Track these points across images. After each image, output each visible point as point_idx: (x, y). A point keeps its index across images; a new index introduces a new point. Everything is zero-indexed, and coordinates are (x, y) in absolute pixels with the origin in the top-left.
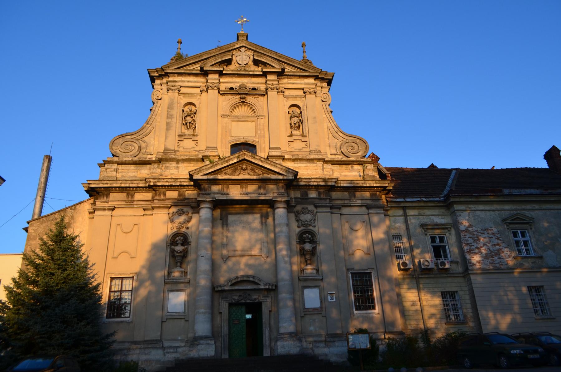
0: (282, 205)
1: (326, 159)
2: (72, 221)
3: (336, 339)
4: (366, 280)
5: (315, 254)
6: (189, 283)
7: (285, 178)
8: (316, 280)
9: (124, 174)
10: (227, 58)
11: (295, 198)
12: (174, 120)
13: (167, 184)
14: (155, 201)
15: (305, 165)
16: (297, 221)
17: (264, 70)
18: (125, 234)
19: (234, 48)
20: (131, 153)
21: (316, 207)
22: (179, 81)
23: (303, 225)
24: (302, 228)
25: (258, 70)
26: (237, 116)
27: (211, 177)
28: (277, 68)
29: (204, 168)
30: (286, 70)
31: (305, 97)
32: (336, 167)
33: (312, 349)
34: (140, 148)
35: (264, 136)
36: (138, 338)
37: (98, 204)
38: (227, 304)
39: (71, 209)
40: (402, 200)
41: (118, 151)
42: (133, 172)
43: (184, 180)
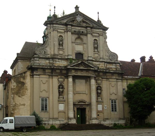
3: (106, 120)
6: (65, 101)
8: (101, 102)
16: (96, 83)
20: (42, 54)
22: (57, 27)
24: (98, 85)
25: (84, 25)
27: (73, 68)
31: (99, 37)
32: (107, 64)
33: (100, 122)
35: (86, 52)
36: (51, 116)
37: (35, 73)
40: (127, 77)
41: (37, 53)
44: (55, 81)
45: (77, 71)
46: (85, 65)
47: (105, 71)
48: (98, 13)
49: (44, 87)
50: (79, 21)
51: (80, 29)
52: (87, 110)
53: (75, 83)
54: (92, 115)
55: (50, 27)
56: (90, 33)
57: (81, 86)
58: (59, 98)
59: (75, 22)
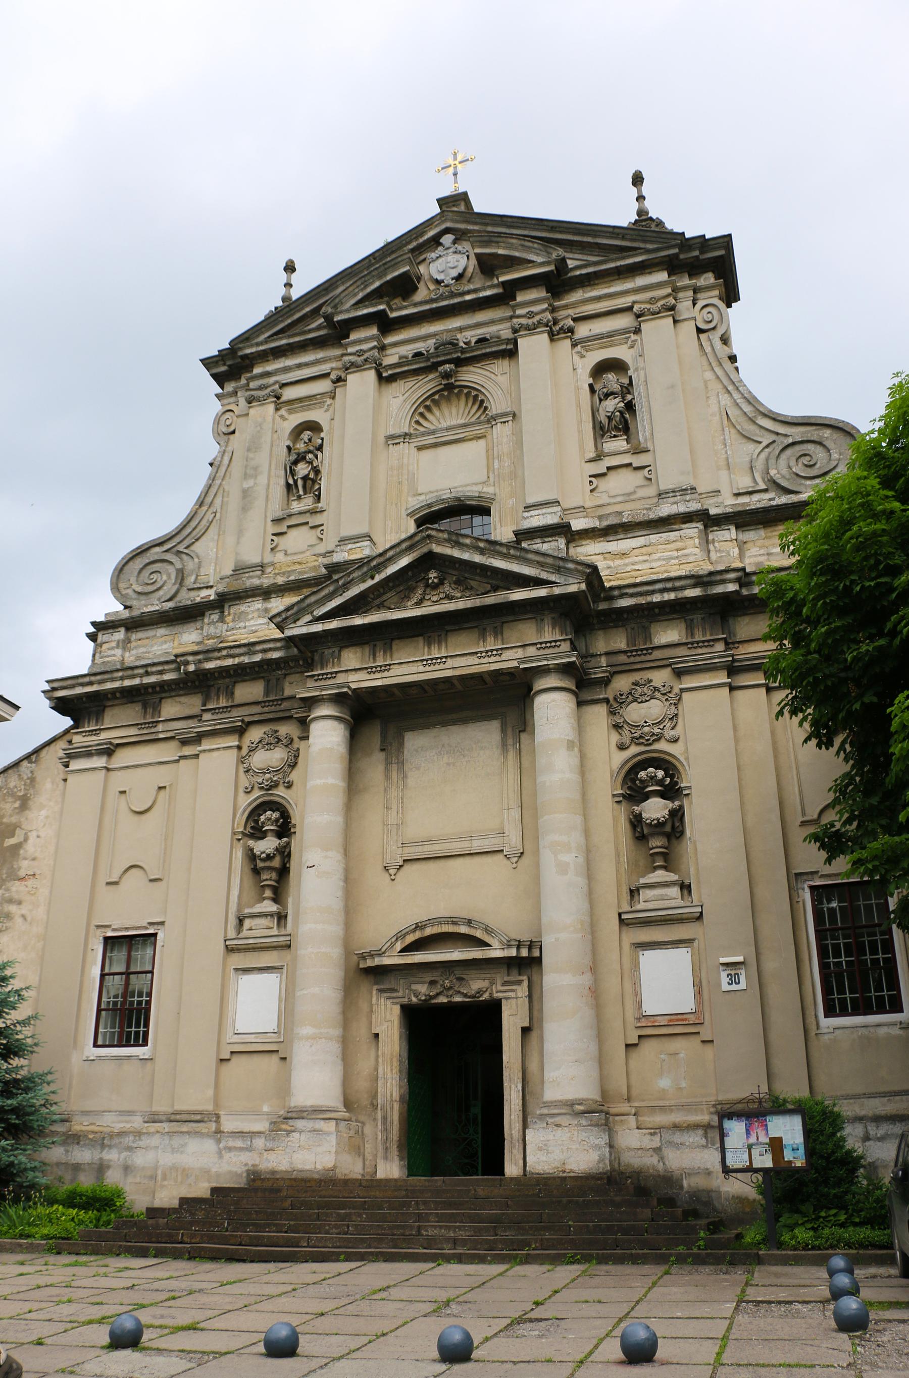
0: (552, 681)
1: (713, 511)
2: (32, 791)
4: (868, 908)
5: (682, 833)
7: (557, 591)
10: (396, 273)
11: (607, 654)
12: (263, 480)
13: (229, 662)
14: (207, 716)
15: (641, 541)
16: (617, 727)
17: (502, 279)
18: (137, 817)
19: (421, 240)
20: (161, 593)
23: (635, 740)
26: (433, 432)
27: (334, 624)
28: (540, 262)
29: (313, 599)
30: (571, 264)
31: (637, 331)
32: (750, 535)
33: (657, 1150)
34: (181, 575)
36: (162, 1107)
38: (397, 1010)
39: (31, 762)
41: (130, 591)
42: (162, 644)
43: (271, 645)
44: (214, 782)
45: (388, 649)
46: (458, 582)
48: (638, 179)
49: (136, 840)
50: (448, 278)
51: (461, 329)
52: (512, 1020)
53: (401, 763)
56: (539, 322)
57: (451, 782)
59: (422, 294)
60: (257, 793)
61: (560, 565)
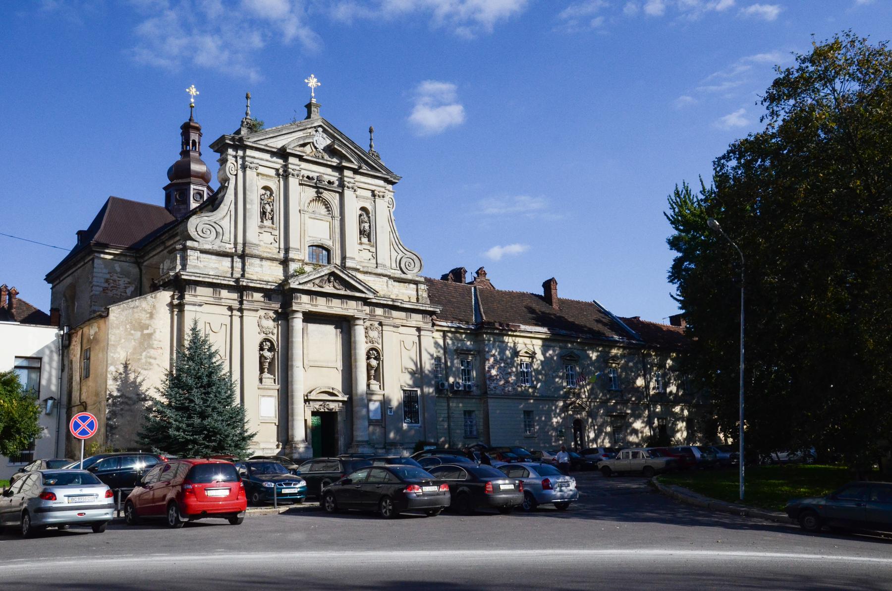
9: (206, 264)
13: (258, 286)
17: (344, 164)
21: (381, 324)
25: (335, 161)
37: (188, 298)
47: (391, 303)
48: (371, 131)
54: (355, 433)
55: (236, 157)
58: (261, 380)
59: (308, 149)
60: (263, 336)
61: (370, 289)
